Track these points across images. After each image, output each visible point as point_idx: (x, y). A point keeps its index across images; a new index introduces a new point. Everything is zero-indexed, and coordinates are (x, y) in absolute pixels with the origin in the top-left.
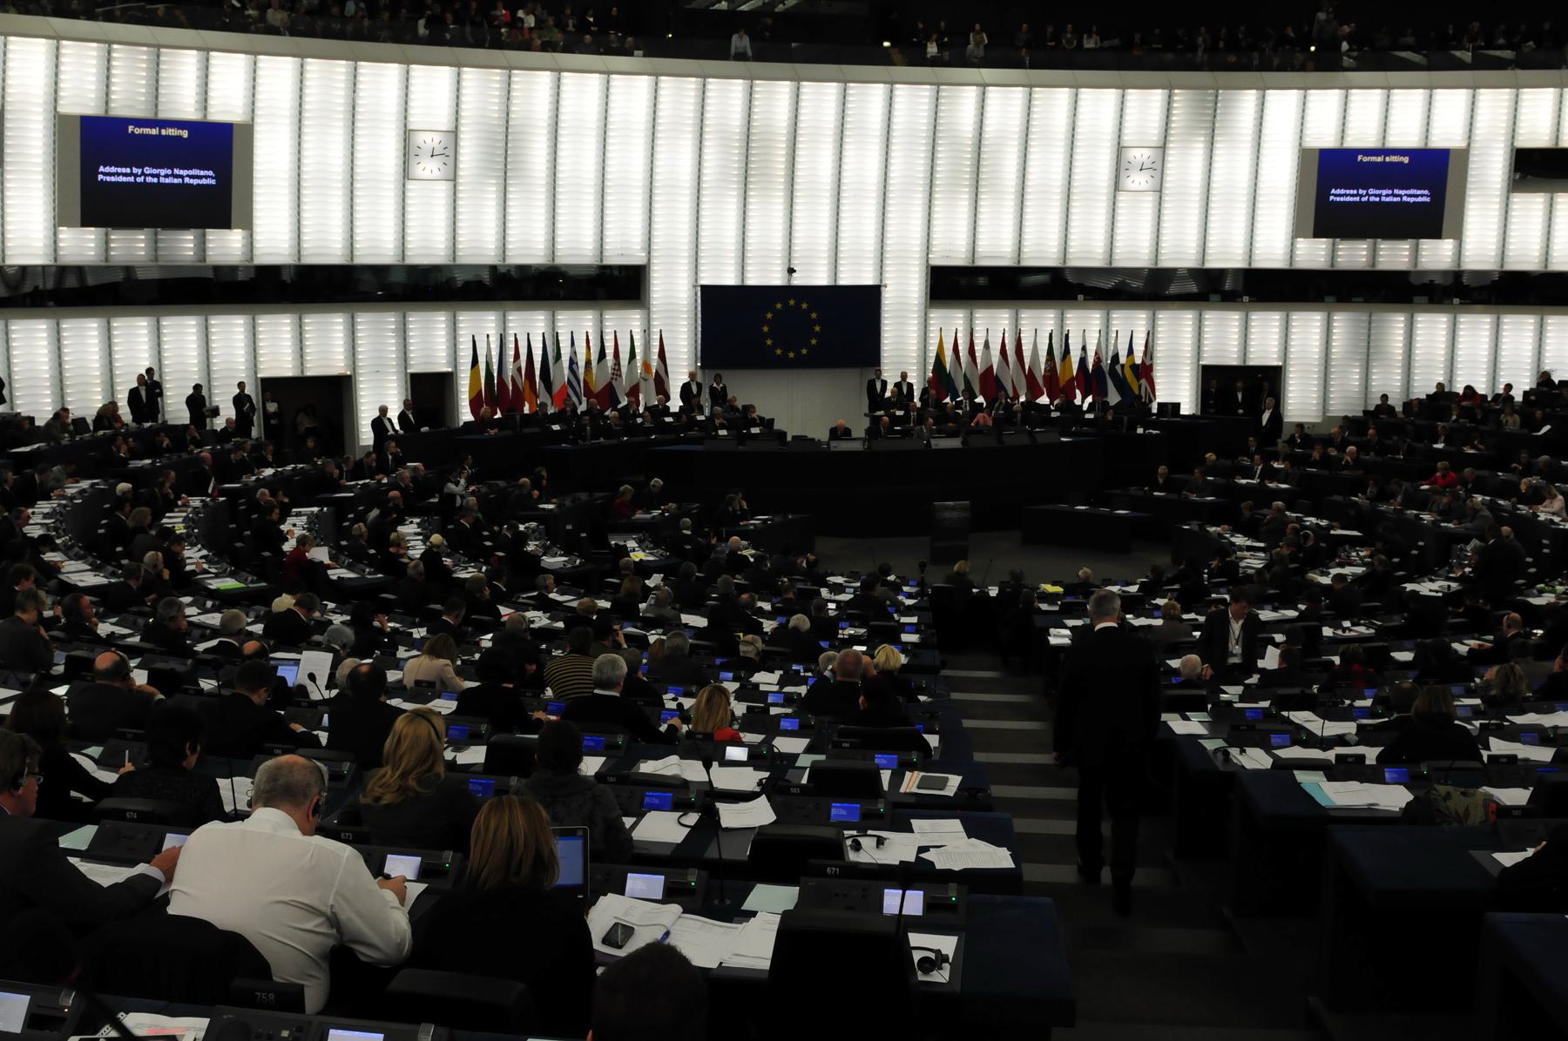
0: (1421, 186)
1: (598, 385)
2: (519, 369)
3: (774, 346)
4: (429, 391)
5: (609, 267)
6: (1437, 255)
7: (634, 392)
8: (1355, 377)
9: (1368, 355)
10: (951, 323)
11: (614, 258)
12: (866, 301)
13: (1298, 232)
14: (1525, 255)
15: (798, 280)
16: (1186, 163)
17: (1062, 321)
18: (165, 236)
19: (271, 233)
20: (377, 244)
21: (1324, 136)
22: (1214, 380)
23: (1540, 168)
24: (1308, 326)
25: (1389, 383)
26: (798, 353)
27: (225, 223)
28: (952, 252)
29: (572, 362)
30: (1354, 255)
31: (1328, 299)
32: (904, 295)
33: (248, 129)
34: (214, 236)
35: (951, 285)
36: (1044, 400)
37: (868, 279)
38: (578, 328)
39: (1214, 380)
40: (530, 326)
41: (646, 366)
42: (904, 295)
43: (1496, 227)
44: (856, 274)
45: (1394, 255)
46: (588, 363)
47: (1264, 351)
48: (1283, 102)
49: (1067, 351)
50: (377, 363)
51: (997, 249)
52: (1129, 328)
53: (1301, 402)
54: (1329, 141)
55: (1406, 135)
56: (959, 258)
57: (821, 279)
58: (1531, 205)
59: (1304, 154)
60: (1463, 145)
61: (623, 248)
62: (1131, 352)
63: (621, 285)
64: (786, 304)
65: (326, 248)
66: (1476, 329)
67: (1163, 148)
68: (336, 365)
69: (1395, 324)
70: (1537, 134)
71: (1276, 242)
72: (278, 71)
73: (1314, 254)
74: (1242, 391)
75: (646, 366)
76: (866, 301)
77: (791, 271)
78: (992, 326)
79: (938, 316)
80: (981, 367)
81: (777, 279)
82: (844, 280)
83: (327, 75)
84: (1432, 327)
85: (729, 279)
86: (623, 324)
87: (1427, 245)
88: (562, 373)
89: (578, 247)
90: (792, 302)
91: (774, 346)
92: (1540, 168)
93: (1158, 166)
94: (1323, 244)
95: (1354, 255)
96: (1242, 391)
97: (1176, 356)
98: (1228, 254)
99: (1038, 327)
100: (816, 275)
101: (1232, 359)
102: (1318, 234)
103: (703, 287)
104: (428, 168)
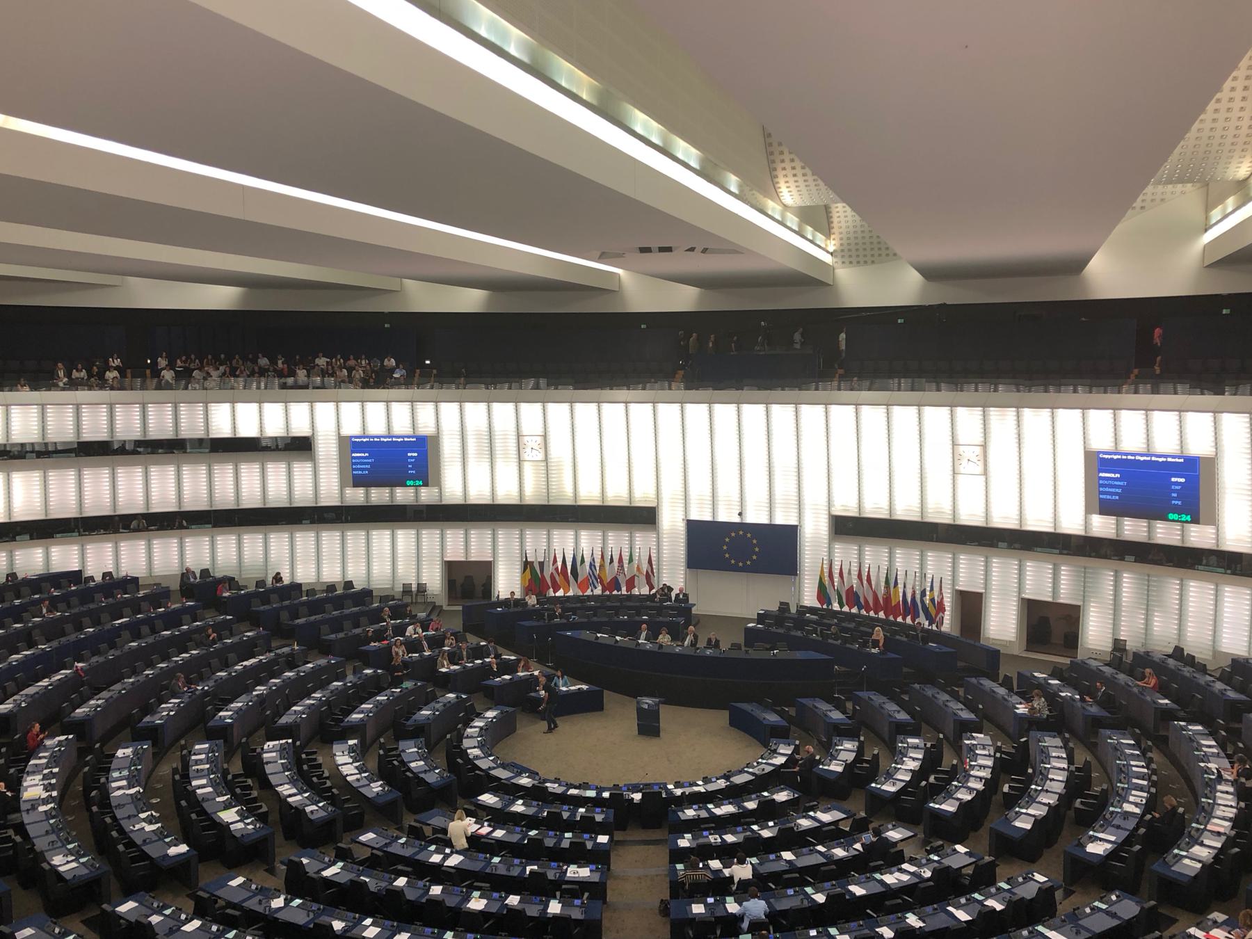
0: (1175, 487)
1: (608, 578)
2: (557, 569)
3: (730, 558)
6: (1199, 536)
7: (631, 584)
13: (1089, 511)
21: (1102, 442)
26: (745, 563)
28: (846, 506)
29: (592, 565)
31: (1127, 558)
32: (814, 530)
34: (423, 490)
35: (847, 527)
36: (882, 615)
37: (793, 522)
38: (617, 541)
41: (638, 569)
42: (814, 530)
44: (783, 518)
46: (602, 566)
48: (1069, 418)
49: (896, 583)
51: (876, 507)
53: (1096, 633)
56: (853, 512)
57: (763, 519)
62: (932, 589)
64: (737, 534)
67: (984, 446)
69: (1170, 583)
71: (1073, 518)
72: (449, 410)
75: (638, 569)
79: (838, 547)
80: (847, 587)
83: (476, 412)
85: (707, 517)
86: (642, 541)
88: (584, 571)
89: (617, 495)
91: (730, 558)
93: (981, 458)
98: (1038, 522)
100: (756, 515)
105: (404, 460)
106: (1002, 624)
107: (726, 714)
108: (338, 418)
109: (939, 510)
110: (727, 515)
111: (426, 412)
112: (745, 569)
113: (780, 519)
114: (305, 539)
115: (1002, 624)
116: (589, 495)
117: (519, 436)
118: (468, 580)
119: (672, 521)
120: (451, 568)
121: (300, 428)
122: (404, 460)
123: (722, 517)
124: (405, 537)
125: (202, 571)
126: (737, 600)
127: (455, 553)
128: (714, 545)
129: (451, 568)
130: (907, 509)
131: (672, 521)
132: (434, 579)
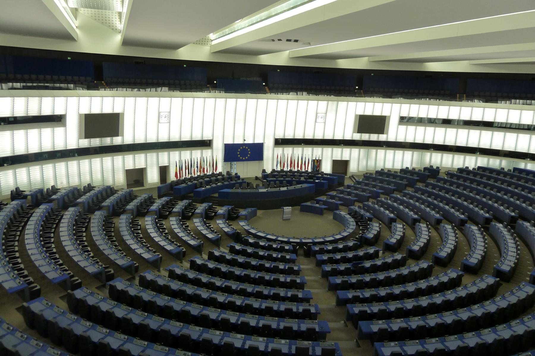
4: (164, 171)
5: (204, 140)
6: (382, 138)
8: (364, 163)
9: (368, 157)
10: (279, 150)
11: (205, 138)
13: (354, 132)
14: (401, 139)
15: (246, 142)
16: (331, 115)
18: (103, 139)
19: (128, 137)
20: (152, 139)
22: (336, 163)
23: (404, 120)
25: (371, 164)
27: (117, 135)
28: (280, 136)
30: (365, 137)
33: (123, 114)
34: (115, 139)
37: (260, 141)
38: (197, 154)
39: (336, 163)
40: (186, 155)
43: (395, 132)
44: (258, 141)
45: (374, 137)
47: (346, 158)
50: (151, 164)
51: (289, 135)
52: (317, 152)
53: (353, 168)
54: (362, 113)
55: (377, 113)
58: (403, 128)
59: (356, 115)
63: (206, 144)
65: (140, 139)
66: (390, 153)
68: (143, 166)
69: (373, 151)
70: (404, 114)
71: (350, 134)
72: (130, 100)
73: (357, 137)
74: (341, 166)
77: (245, 140)
78: (288, 151)
79: (275, 149)
81: (241, 142)
82: (255, 142)
83: (141, 101)
84: (381, 152)
86: (207, 153)
87: (380, 135)
89: (197, 137)
92: (404, 120)
94: (359, 134)
95: (365, 137)
96: (341, 166)
97: (327, 158)
98: (339, 136)
99: (298, 151)
100: (249, 141)
101: (339, 158)
102: (358, 132)
104: (163, 120)
105: (101, 125)
106: (327, 168)
107: (299, 207)
108: (76, 104)
109: (309, 136)
111: (119, 100)
112: (246, 160)
113: (257, 141)
114: (61, 166)
115: (327, 168)
116: (186, 137)
117: (159, 113)
118: (136, 177)
120: (129, 173)
121: (58, 112)
122: (101, 125)
123: (236, 142)
124: (108, 160)
125: (52, 186)
126: (246, 170)
127: (130, 166)
128: (233, 152)
129: (129, 173)
130: (299, 135)
132: (120, 180)
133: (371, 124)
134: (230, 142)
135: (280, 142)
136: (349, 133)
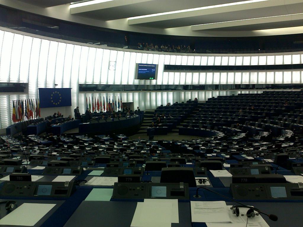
6: (154, 82)
8: (143, 104)
9: (145, 100)
12: (69, 90)
17: (114, 95)
24: (136, 95)
28: (82, 82)
32: (75, 89)
42: (75, 89)
44: (66, 86)
60: (158, 64)
61: (23, 80)
73: (137, 82)
76: (69, 90)
90: (56, 92)
95: (142, 82)
103: (40, 89)
110: (51, 86)
119: (33, 90)
131: (33, 90)
133: (146, 72)
134: (42, 86)
135: (84, 88)
136: (130, 79)
